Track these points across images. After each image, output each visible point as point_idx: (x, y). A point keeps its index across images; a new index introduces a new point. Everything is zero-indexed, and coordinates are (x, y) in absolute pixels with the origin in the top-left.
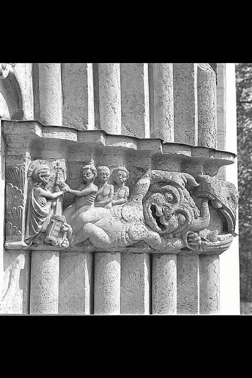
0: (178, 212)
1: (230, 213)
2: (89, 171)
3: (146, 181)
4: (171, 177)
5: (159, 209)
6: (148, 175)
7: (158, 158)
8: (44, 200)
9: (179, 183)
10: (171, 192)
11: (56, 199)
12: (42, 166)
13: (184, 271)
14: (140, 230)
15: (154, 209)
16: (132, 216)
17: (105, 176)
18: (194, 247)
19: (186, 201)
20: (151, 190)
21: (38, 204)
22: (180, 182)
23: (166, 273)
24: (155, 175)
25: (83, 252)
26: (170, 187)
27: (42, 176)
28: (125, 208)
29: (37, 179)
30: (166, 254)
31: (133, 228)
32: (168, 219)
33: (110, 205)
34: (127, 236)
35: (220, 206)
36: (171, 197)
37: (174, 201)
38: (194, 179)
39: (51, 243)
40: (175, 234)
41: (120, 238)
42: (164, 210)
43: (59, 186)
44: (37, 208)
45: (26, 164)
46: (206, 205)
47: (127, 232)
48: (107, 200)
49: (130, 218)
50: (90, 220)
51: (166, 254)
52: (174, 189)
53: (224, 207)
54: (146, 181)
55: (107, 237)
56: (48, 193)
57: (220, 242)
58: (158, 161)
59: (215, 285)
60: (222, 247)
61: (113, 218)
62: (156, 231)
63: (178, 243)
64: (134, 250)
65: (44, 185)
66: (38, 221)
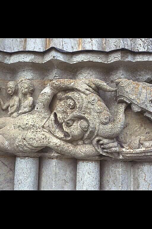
0: (80, 118)
4: (73, 84)
7: (76, 70)
9: (80, 89)
13: (110, 177)
15: (55, 115)
16: (30, 123)
18: (112, 153)
24: (54, 83)
26: (70, 94)
31: (29, 134)
33: (15, 114)
35: (136, 109)
36: (71, 104)
41: (17, 145)
42: (63, 117)
46: (122, 108)
47: (24, 139)
49: (27, 126)
52: (76, 95)
60: (149, 154)
61: (13, 126)
62: (57, 137)
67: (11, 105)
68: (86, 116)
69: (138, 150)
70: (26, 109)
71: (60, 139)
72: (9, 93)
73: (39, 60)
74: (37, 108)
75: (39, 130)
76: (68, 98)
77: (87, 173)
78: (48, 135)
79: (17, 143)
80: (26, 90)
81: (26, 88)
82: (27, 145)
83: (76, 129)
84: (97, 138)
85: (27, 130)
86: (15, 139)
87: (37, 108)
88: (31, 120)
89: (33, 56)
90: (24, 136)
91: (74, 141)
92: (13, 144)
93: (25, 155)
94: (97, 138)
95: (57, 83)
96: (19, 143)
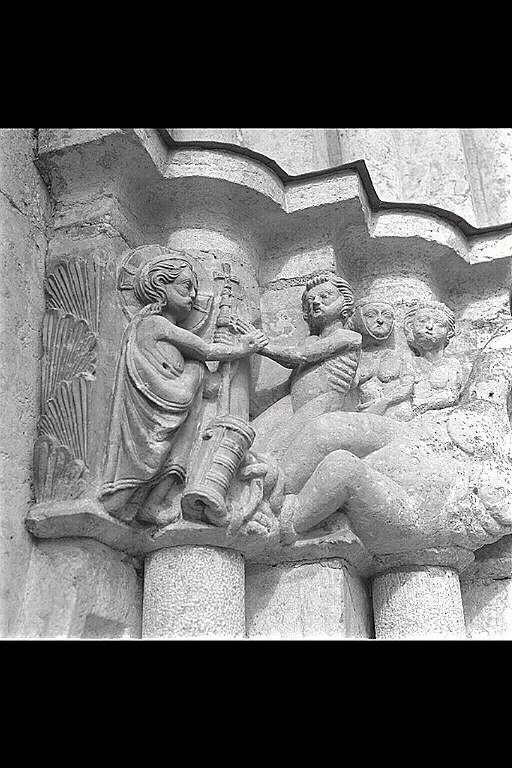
25: (334, 554)
33: (405, 406)
39: (199, 509)
41: (456, 509)
43: (232, 330)
44: (146, 377)
50: (344, 439)
61: (423, 444)
66: (151, 424)
67: (388, 373)
70: (448, 395)
72: (381, 331)
74: (491, 395)
79: (451, 502)
81: (444, 326)
82: (483, 513)
85: (482, 459)
86: (444, 488)
87: (491, 395)
89: (454, 236)
92: (437, 506)
96: (462, 505)
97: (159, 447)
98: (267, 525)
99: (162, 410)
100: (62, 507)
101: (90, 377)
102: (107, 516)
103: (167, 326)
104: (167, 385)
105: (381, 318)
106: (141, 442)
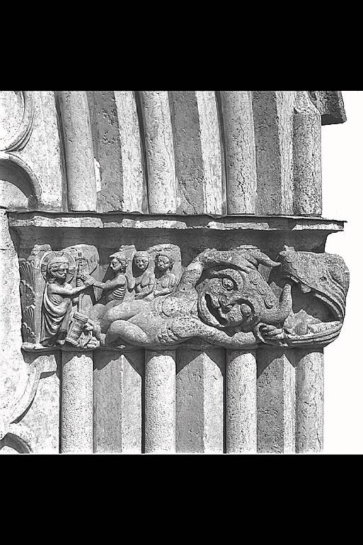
0: (240, 302)
1: (328, 297)
2: (115, 260)
3: (197, 266)
4: (230, 259)
5: (215, 299)
6: (198, 259)
8: (58, 298)
10: (229, 277)
11: (77, 294)
12: (61, 260)
14: (189, 326)
17: (142, 263)
19: (254, 287)
20: (206, 274)
21: (49, 303)
22: (243, 264)
23: (237, 373)
24: (206, 258)
25: (121, 352)
26: (227, 271)
27: (54, 271)
28: (168, 300)
29: (51, 275)
30: (237, 350)
32: (226, 310)
33: (151, 296)
34: (172, 334)
35: (306, 290)
37: (235, 287)
38: (268, 259)
40: (244, 326)
41: (161, 336)
44: (49, 308)
45: (37, 259)
46: (288, 288)
48: (146, 290)
50: (118, 317)
51: (237, 350)
53: (314, 291)
54: (197, 266)
55: (144, 335)
56: (69, 288)
57: (313, 334)
58: (225, 240)
59: (312, 386)
60: (317, 340)
61: (151, 313)
62: (211, 325)
63: (248, 337)
64: (192, 346)
65: (61, 282)
66: (53, 321)
67: (144, 284)
68: (249, 299)
69: (306, 336)
71: (216, 327)
73: (183, 226)
75: (187, 317)
76: (222, 277)
77: (244, 366)
78: (199, 322)
80: (167, 265)
83: (236, 313)
84: (260, 324)
88: (176, 303)
90: (170, 326)
91: (230, 328)
92: (155, 335)
93: (160, 348)
94: (260, 324)
95: (209, 258)
97: (55, 327)
98: (95, 343)
99: (55, 317)
100: (30, 346)
101: (34, 307)
102: (42, 347)
103: (56, 287)
104: (55, 309)
105: (142, 263)
106: (50, 326)
